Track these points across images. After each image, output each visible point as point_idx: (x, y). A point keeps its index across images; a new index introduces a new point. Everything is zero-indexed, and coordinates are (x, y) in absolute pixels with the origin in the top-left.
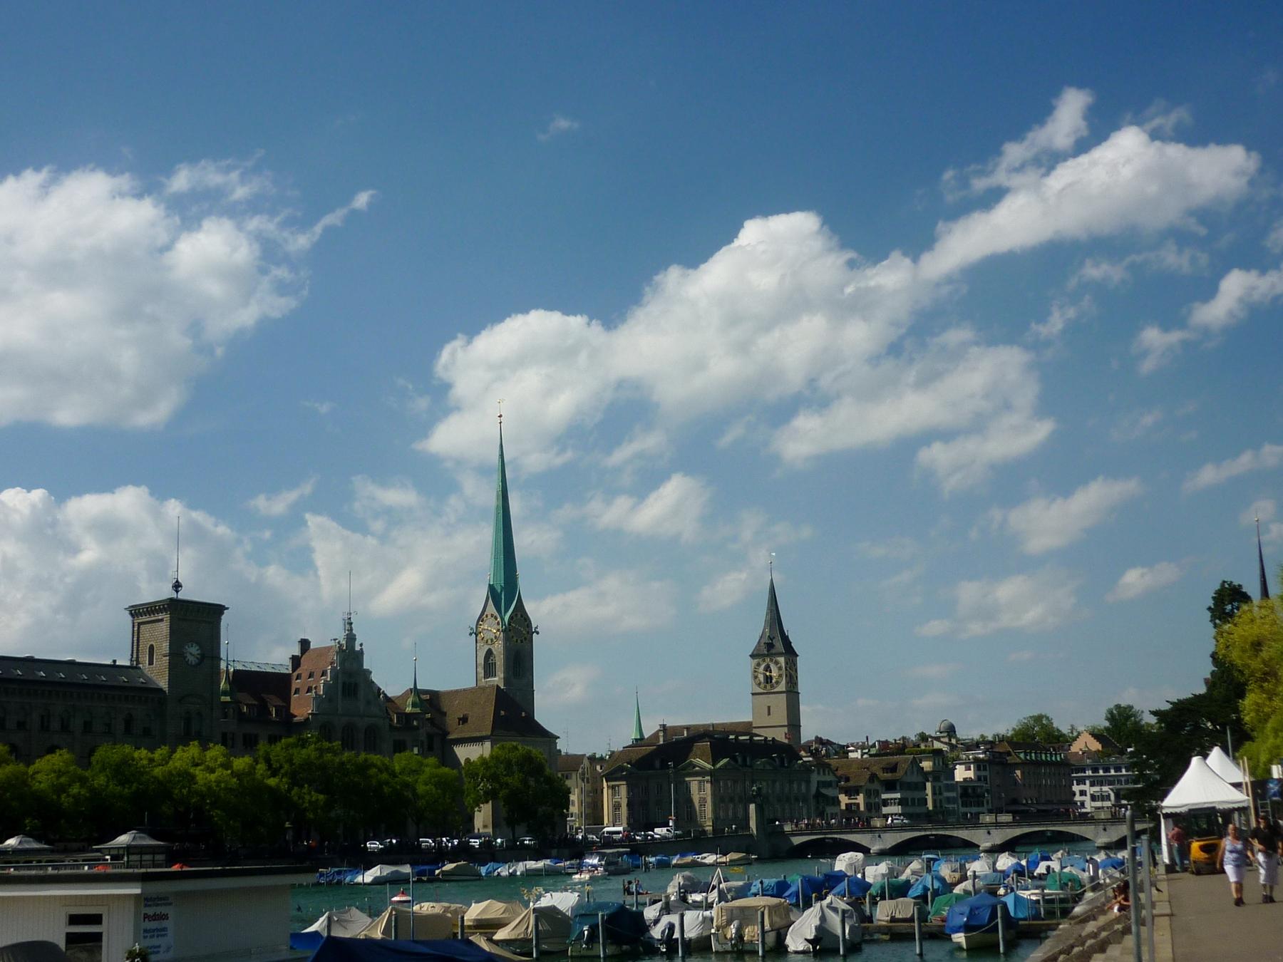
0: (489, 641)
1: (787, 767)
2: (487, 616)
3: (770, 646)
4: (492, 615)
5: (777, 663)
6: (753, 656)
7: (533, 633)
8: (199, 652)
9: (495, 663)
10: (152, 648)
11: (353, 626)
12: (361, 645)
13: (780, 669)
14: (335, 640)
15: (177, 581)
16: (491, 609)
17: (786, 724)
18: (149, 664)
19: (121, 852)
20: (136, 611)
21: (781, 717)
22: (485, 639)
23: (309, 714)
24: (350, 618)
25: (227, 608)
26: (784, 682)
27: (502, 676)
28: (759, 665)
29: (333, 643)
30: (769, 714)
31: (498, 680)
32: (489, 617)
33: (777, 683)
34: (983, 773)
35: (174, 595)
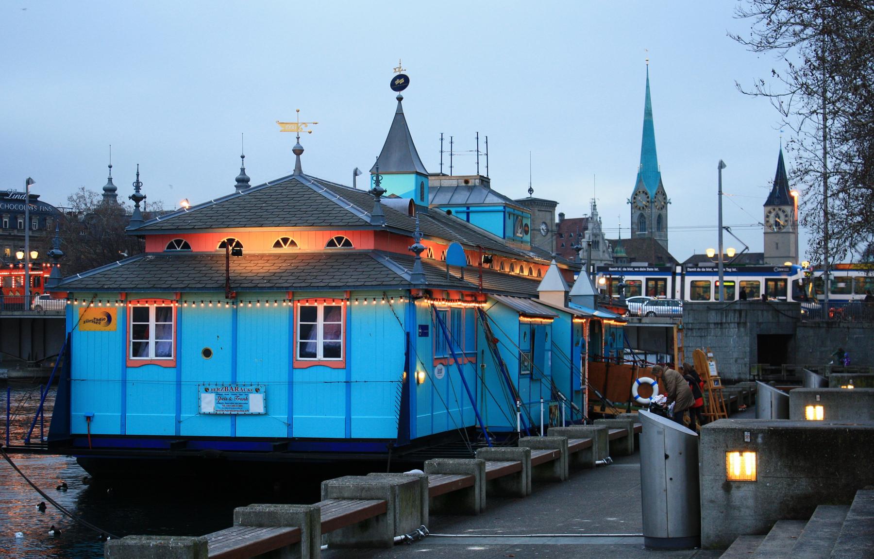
0: (641, 208)
2: (639, 192)
5: (784, 212)
12: (600, 218)
14: (585, 215)
15: (531, 188)
22: (638, 207)
28: (770, 212)
29: (584, 217)
30: (777, 248)
32: (641, 192)
35: (529, 195)
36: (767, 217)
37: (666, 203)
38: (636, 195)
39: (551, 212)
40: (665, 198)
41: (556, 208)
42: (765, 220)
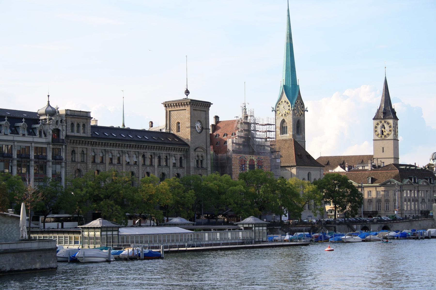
0: (283, 115)
1: (433, 184)
2: (282, 102)
4: (285, 101)
5: (388, 124)
6: (374, 119)
7: (305, 111)
8: (200, 126)
9: (287, 127)
10: (178, 123)
13: (390, 127)
14: (237, 117)
15: (187, 90)
16: (285, 98)
17: (393, 157)
18: (177, 132)
19: (251, 226)
20: (167, 105)
21: (390, 153)
24: (245, 106)
25: (212, 104)
27: (291, 133)
28: (378, 124)
29: (236, 119)
30: (383, 151)
31: (289, 135)
32: (283, 102)
35: (186, 97)
36: (376, 127)
37: (304, 111)
38: (279, 104)
39: (205, 111)
40: (303, 107)
41: (210, 108)
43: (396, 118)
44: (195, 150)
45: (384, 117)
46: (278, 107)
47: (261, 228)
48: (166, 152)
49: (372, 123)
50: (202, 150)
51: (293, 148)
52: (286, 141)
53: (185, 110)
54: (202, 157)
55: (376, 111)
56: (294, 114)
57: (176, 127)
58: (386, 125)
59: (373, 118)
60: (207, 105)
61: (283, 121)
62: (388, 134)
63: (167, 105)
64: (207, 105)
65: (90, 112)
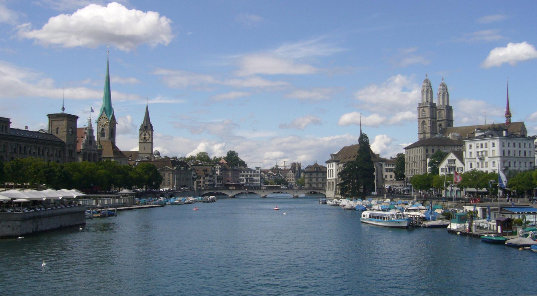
0: (103, 126)
2: (102, 117)
3: (146, 127)
4: (105, 117)
5: (148, 133)
6: (140, 130)
9: (105, 133)
10: (58, 128)
11: (92, 122)
12: (93, 128)
13: (149, 135)
14: (85, 126)
15: (63, 107)
16: (104, 115)
18: (56, 134)
19: (127, 195)
20: (50, 116)
22: (101, 125)
23: (81, 150)
24: (91, 119)
25: (79, 117)
26: (151, 139)
27: (108, 137)
28: (142, 133)
29: (84, 127)
30: (145, 149)
31: (106, 138)
33: (148, 139)
34: (221, 172)
35: (62, 112)
36: (141, 135)
40: (115, 121)
41: (78, 120)
42: (139, 136)
43: (152, 130)
44: (69, 146)
45: (146, 129)
46: (100, 120)
47: (133, 196)
48: (51, 147)
49: (138, 132)
50: (72, 146)
51: (111, 146)
52: (106, 141)
53: (63, 120)
54: (72, 150)
55: (141, 125)
56: (110, 125)
57: (56, 131)
58: (147, 134)
59: (139, 129)
60: (76, 118)
61: (103, 129)
62: (148, 139)
63: (50, 116)
64: (76, 118)
65: (10, 119)
